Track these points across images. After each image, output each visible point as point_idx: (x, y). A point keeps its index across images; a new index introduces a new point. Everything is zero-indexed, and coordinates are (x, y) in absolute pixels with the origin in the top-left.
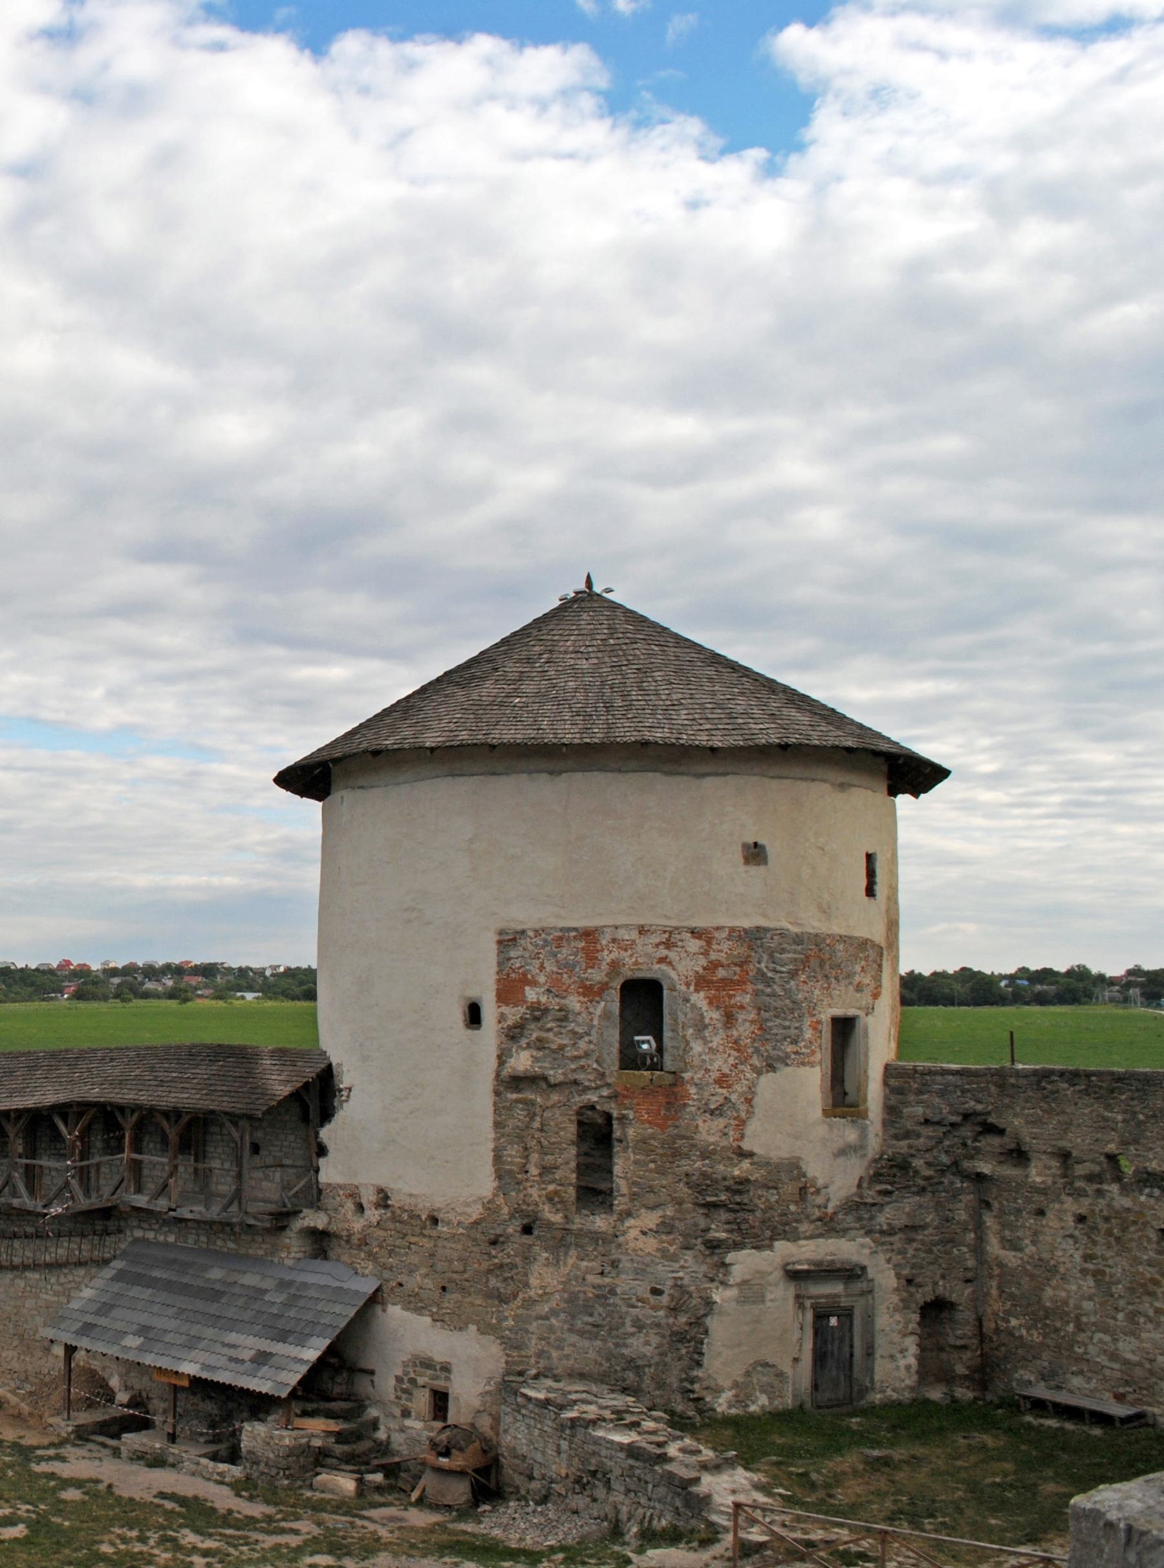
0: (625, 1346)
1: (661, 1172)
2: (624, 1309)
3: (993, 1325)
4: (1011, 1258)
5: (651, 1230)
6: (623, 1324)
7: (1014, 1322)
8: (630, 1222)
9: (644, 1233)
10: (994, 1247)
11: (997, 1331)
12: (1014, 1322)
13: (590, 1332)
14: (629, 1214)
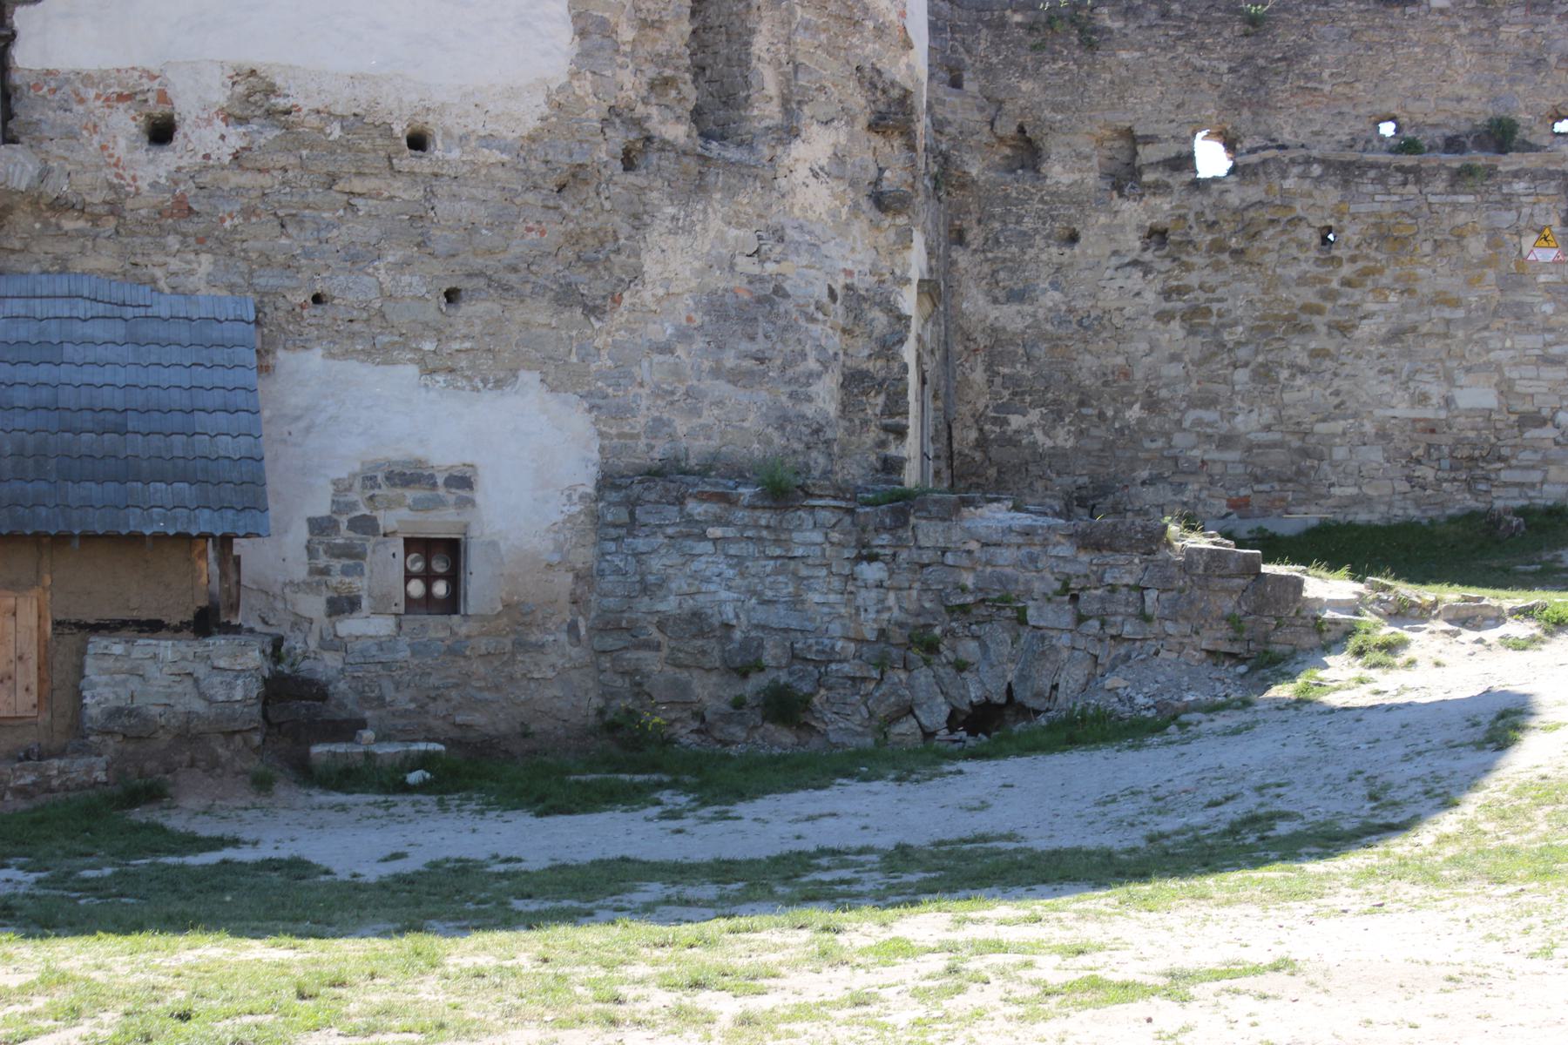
0: (809, 399)
1: (832, 50)
2: (802, 322)
3: (973, 435)
4: (1011, 317)
5: (822, 169)
6: (804, 356)
7: (1016, 421)
8: (798, 149)
9: (816, 175)
10: (975, 304)
11: (982, 443)
12: (1016, 421)
13: (750, 373)
14: (789, 132)
